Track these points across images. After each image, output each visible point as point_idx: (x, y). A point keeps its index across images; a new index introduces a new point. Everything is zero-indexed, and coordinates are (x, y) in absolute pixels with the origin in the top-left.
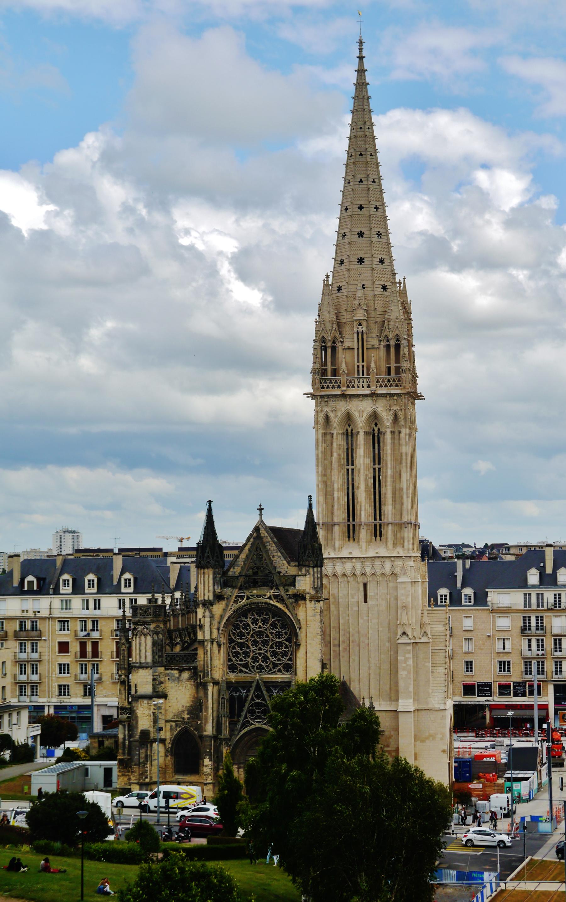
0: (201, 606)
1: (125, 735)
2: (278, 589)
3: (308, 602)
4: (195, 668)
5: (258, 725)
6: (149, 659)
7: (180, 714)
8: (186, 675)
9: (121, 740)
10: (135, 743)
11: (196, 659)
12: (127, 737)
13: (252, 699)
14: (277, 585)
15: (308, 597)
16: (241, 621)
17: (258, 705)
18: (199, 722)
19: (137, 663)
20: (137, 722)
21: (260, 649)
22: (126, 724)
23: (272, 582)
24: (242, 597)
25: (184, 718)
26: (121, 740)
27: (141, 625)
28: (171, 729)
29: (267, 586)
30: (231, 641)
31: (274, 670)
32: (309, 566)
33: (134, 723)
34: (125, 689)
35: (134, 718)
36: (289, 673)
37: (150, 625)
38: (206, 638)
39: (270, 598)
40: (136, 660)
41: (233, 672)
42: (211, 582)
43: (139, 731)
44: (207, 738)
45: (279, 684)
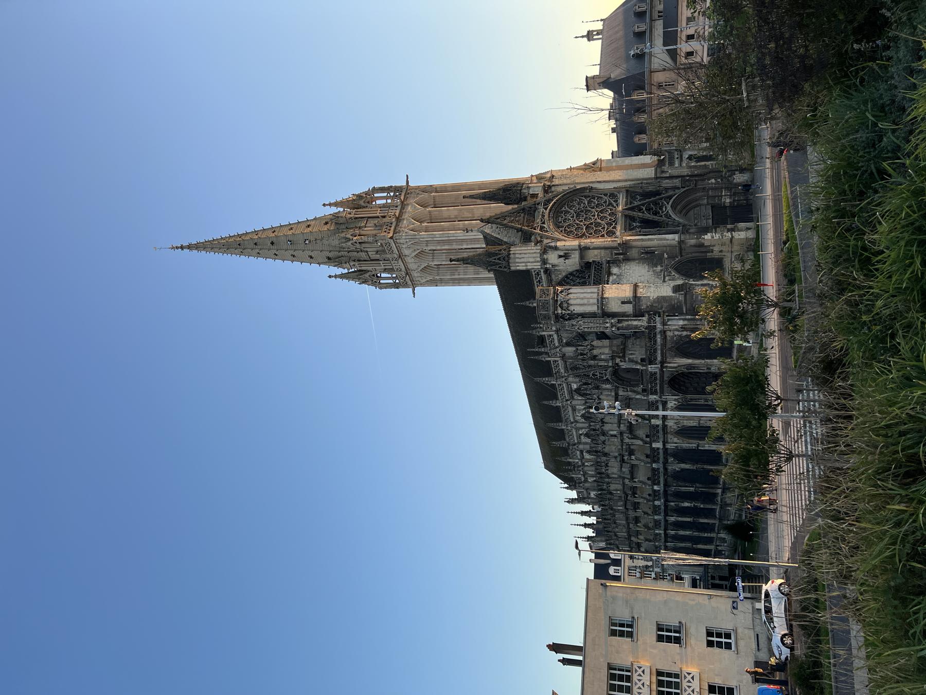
0: (545, 256)
1: (680, 319)
2: (538, 204)
3: (553, 183)
4: (608, 262)
5: (669, 207)
6: (596, 290)
7: (657, 273)
8: (615, 270)
9: (686, 322)
10: (688, 302)
11: (599, 263)
12: (682, 317)
13: (643, 213)
14: (535, 204)
15: (549, 184)
16: (565, 230)
17: (648, 210)
18: (666, 256)
19: (598, 299)
20: (664, 298)
21: (594, 216)
22: (666, 318)
23: (530, 208)
24: (542, 228)
25: (661, 270)
26: (686, 322)
27: (557, 297)
28: (673, 280)
29: (535, 211)
30: (583, 236)
31: (615, 205)
32: (522, 187)
33: (665, 305)
34: (627, 320)
35: (660, 306)
36: (618, 194)
37: (558, 290)
38: (577, 247)
39: (546, 209)
40: (595, 304)
41: (614, 233)
42: (523, 248)
43: (673, 295)
44: (682, 237)
45: (629, 201)
